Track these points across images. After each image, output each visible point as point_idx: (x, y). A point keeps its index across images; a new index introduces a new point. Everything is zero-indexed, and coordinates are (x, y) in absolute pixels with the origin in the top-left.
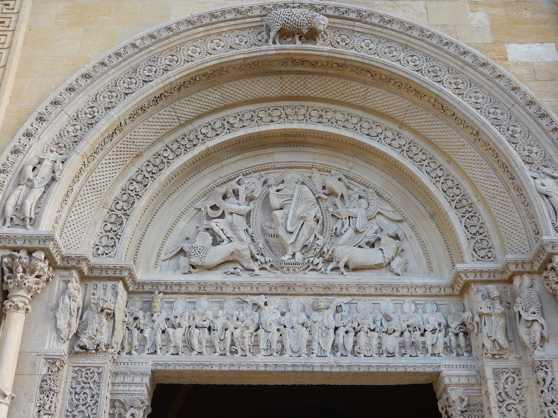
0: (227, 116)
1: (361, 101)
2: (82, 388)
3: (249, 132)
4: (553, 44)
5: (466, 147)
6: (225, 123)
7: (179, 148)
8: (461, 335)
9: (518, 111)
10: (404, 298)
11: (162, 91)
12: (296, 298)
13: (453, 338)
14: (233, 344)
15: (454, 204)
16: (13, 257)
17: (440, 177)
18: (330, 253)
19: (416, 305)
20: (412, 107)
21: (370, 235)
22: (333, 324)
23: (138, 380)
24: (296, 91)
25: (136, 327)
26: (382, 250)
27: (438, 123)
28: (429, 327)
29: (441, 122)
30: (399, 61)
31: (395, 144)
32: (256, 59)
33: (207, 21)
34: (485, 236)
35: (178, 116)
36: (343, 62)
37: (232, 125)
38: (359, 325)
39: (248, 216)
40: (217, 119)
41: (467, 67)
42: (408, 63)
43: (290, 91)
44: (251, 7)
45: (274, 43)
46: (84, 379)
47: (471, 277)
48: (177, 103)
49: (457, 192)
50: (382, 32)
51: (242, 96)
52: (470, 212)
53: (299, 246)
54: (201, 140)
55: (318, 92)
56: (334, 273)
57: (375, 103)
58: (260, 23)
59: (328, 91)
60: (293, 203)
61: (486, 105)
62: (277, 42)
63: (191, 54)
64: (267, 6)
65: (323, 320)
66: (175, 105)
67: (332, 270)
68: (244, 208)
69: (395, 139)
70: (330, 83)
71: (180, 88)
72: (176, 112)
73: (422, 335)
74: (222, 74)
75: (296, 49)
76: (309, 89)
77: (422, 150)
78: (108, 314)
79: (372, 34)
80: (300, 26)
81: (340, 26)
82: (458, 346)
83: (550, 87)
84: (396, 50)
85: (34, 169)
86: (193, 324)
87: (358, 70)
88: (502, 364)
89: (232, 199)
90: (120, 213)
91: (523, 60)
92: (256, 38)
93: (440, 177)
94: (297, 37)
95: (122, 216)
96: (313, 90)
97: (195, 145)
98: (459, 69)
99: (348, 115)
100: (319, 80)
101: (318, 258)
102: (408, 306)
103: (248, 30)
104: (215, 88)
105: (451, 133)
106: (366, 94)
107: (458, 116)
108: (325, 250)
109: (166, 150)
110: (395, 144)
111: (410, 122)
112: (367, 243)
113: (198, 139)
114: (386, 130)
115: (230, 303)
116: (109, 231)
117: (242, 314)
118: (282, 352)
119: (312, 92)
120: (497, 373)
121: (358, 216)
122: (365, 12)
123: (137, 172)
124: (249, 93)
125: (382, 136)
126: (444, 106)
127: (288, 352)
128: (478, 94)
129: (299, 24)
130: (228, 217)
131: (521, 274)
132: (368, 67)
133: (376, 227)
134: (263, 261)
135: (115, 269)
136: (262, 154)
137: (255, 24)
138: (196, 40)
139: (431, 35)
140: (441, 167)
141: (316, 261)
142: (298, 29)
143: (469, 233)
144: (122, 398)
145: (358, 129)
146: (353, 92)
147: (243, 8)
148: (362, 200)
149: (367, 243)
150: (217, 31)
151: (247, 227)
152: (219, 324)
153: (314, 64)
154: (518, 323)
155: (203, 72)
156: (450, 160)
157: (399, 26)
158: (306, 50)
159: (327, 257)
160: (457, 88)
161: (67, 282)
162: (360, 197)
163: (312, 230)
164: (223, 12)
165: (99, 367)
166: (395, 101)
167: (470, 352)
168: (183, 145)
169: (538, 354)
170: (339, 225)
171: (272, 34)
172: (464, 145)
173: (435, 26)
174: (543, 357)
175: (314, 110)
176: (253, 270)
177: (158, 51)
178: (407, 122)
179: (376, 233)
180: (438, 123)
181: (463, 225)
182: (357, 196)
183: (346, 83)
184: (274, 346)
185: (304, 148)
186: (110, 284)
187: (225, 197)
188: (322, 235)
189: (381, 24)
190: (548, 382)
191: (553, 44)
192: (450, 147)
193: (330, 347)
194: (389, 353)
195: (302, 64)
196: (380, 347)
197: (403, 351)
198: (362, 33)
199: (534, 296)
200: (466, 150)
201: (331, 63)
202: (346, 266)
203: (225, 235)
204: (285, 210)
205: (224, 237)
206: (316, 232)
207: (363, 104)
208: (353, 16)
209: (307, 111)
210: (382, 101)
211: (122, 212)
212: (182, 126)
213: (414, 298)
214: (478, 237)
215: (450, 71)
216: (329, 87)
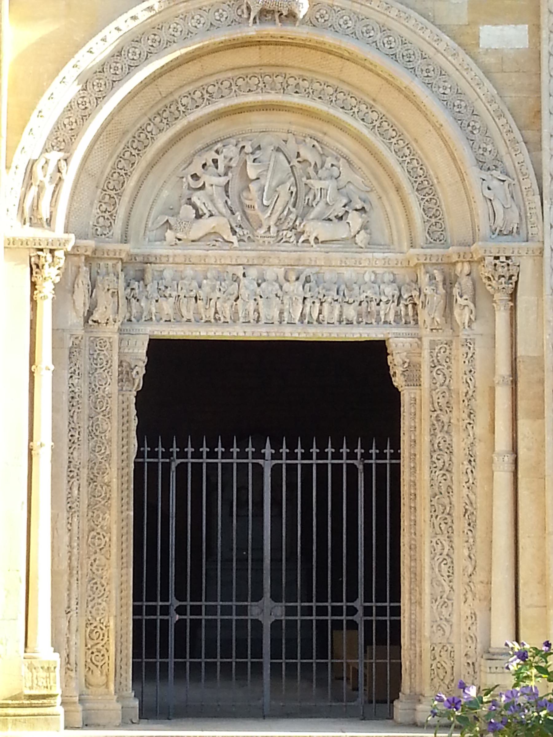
2: (99, 354)
4: (527, 26)
6: (205, 92)
8: (410, 306)
9: (480, 107)
10: (366, 269)
12: (271, 267)
13: (403, 309)
14: (216, 312)
15: (416, 185)
17: (406, 156)
18: (302, 226)
19: (376, 274)
25: (133, 297)
26: (348, 223)
28: (384, 299)
34: (440, 219)
37: (211, 95)
38: (324, 296)
39: (226, 187)
42: (384, 44)
45: (255, 22)
46: (98, 347)
52: (429, 194)
56: (305, 244)
61: (453, 97)
62: (258, 21)
63: (173, 33)
65: (293, 291)
67: (303, 242)
68: (223, 180)
73: (378, 304)
78: (114, 292)
82: (407, 315)
83: (514, 80)
84: (373, 29)
89: (212, 169)
90: (113, 193)
91: (493, 47)
93: (406, 156)
95: (115, 196)
101: (291, 231)
108: (297, 223)
109: (150, 124)
116: (105, 212)
117: (223, 284)
120: (433, 343)
121: (329, 189)
123: (124, 149)
125: (356, 110)
128: (446, 84)
133: (345, 201)
134: (242, 234)
135: (115, 251)
140: (409, 146)
141: (290, 234)
143: (425, 216)
148: (334, 167)
151: (227, 198)
154: (454, 305)
159: (299, 230)
162: (332, 165)
165: (110, 338)
170: (311, 197)
174: (468, 335)
176: (232, 243)
179: (344, 206)
181: (422, 207)
182: (330, 165)
186: (110, 263)
188: (294, 206)
190: (470, 355)
191: (527, 26)
193: (299, 315)
194: (348, 320)
197: (360, 320)
199: (470, 283)
202: (316, 238)
203: (207, 208)
204: (262, 181)
205: (205, 211)
206: (290, 206)
211: (114, 192)
213: (374, 269)
214: (433, 220)
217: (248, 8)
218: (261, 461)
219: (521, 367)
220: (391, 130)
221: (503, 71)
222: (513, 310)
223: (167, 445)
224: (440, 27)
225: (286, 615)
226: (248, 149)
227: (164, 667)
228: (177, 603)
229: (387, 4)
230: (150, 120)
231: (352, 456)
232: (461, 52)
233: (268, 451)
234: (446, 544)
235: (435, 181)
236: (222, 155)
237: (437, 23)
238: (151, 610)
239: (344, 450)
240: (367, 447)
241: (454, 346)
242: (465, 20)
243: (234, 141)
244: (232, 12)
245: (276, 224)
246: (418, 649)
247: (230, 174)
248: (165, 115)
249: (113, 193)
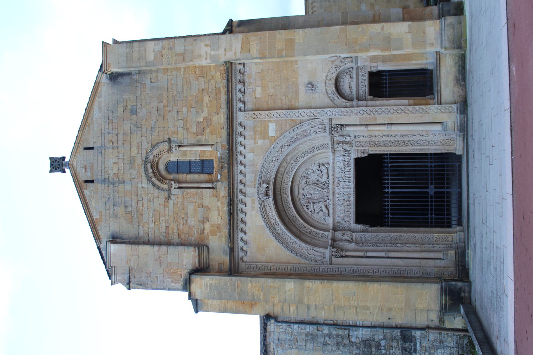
4: (269, 124)
9: (291, 136)
14: (348, 206)
16: (334, 255)
21: (319, 172)
22: (343, 182)
23: (357, 227)
28: (344, 160)
33: (263, 215)
47: (333, 150)
49: (309, 150)
53: (322, 190)
60: (310, 191)
85: (310, 254)
86: (343, 215)
88: (354, 145)
89: (309, 207)
90: (316, 234)
94: (268, 191)
102: (337, 164)
112: (321, 173)
115: (337, 207)
118: (350, 194)
120: (356, 146)
127: (350, 193)
130: (314, 208)
131: (333, 139)
133: (317, 171)
135: (332, 234)
141: (326, 185)
144: (361, 230)
149: (321, 173)
152: (342, 208)
156: (300, 152)
159: (325, 183)
161: (337, 244)
163: (318, 187)
164: (261, 211)
167: (349, 151)
169: (353, 138)
170: (316, 180)
184: (349, 196)
186: (335, 235)
187: (308, 209)
191: (269, 124)
196: (348, 171)
199: (339, 137)
202: (327, 178)
204: (312, 193)
208: (261, 176)
214: (322, 147)
217: (266, 199)
218: (389, 192)
219: (363, 123)
221: (281, 130)
222: (346, 125)
223: (385, 218)
224: (270, 147)
225: (432, 185)
226: (303, 197)
227: (447, 219)
228: (429, 215)
231: (387, 167)
232: (277, 141)
233: (386, 190)
234: (412, 142)
235: (311, 146)
236: (305, 204)
237: (269, 148)
238: (431, 222)
239: (386, 169)
240: (385, 163)
241: (357, 141)
242: (268, 140)
243: (301, 201)
245: (324, 189)
246: (442, 149)
247: (310, 202)
249: (316, 234)
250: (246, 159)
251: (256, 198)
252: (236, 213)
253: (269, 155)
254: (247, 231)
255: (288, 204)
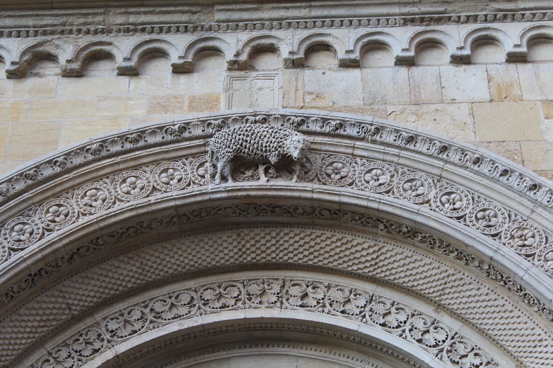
0: (151, 300)
1: (372, 269)
3: (186, 326)
5: (545, 343)
6: (147, 311)
7: (69, 356)
11: (41, 265)
20: (453, 278)
24: (264, 255)
27: (497, 303)
29: (501, 302)
30: (428, 202)
31: (429, 338)
32: (195, 207)
33: (117, 148)
35: (68, 304)
36: (337, 207)
37: (158, 315)
40: (134, 305)
41: (540, 210)
42: (443, 204)
43: (253, 255)
44: (188, 124)
48: (67, 283)
50: (399, 156)
51: (175, 267)
54: (106, 341)
55: (301, 256)
57: (394, 271)
58: (203, 149)
59: (316, 254)
64: (212, 122)
66: (64, 286)
69: (428, 331)
70: (318, 240)
71: (71, 258)
72: (64, 297)
74: (142, 232)
75: (259, 189)
76: (285, 252)
77: (473, 349)
79: (383, 160)
80: (266, 151)
81: (332, 149)
87: (363, 219)
92: (195, 173)
94: (261, 169)
96: (292, 252)
97: (96, 351)
98: (527, 212)
99: (351, 292)
100: (302, 236)
103: (184, 160)
104: (130, 255)
105: (519, 320)
106: (378, 257)
107: (527, 292)
110: (429, 338)
111: (452, 302)
113: (103, 340)
114: (413, 315)
119: (291, 255)
122: (372, 125)
124: (187, 261)
125: (407, 327)
126: (505, 276)
129: (264, 149)
132: (377, 214)
136: (211, 361)
137: (194, 151)
138: (101, 177)
139: (478, 159)
142: (262, 156)
145: (367, 316)
146: (358, 255)
147: (174, 125)
150: (133, 163)
153: (291, 210)
155: (108, 231)
157: (426, 146)
158: (276, 190)
160: (524, 246)
164: (141, 134)
166: (425, 269)
168: (76, 351)
171: (220, 165)
172: (540, 341)
173: (486, 144)
175: (294, 285)
177: (35, 200)
178: (447, 302)
180: (497, 303)
183: (344, 241)
185: (280, 349)
189: (398, 143)
192: (520, 344)
195: (273, 212)
198: (368, 159)
200: (545, 350)
201: (318, 210)
207: (374, 273)
208: (352, 131)
209: (283, 287)
210: (404, 269)
212: (76, 320)
215: (513, 217)
216: (317, 247)
220: (471, 355)
229: (440, 142)
230: (50, 354)
244: (189, 172)
248: (76, 347)
250: (452, 69)
251: (223, 110)
252: (143, 18)
253: (485, 168)
254: (30, 82)
255: (183, 311)
